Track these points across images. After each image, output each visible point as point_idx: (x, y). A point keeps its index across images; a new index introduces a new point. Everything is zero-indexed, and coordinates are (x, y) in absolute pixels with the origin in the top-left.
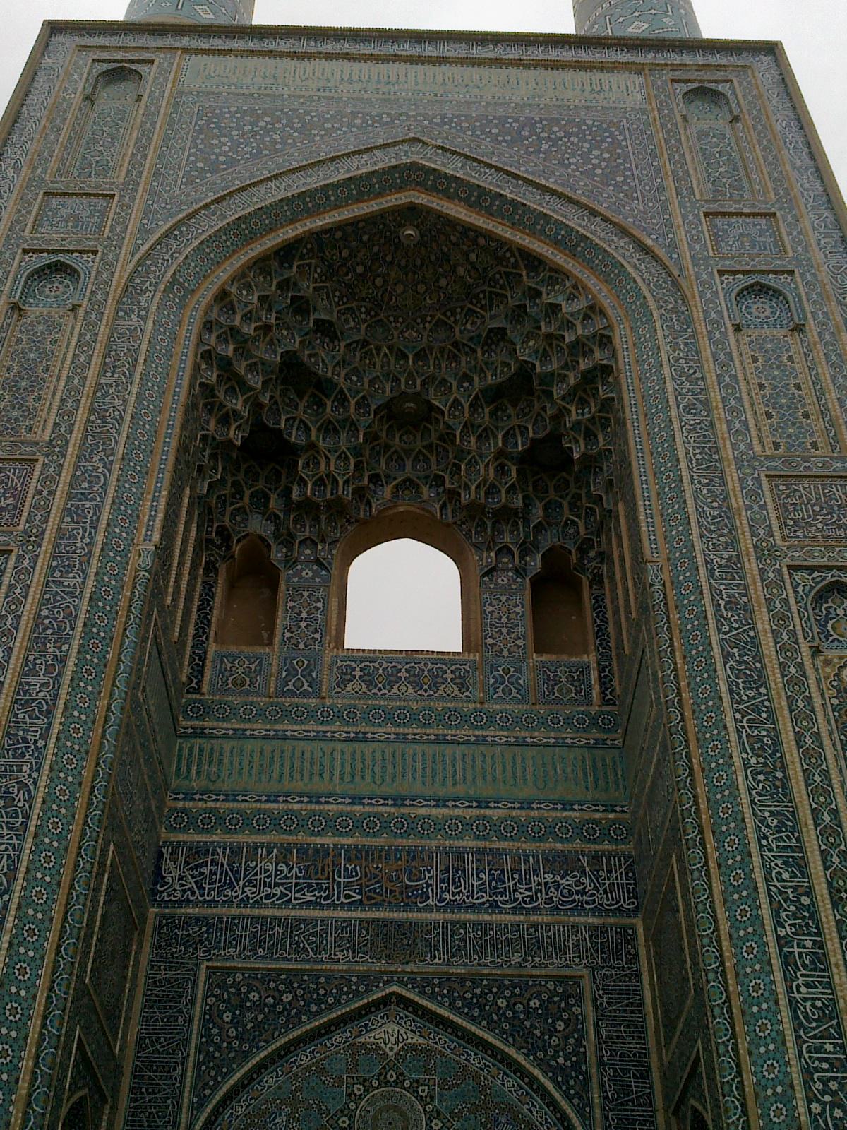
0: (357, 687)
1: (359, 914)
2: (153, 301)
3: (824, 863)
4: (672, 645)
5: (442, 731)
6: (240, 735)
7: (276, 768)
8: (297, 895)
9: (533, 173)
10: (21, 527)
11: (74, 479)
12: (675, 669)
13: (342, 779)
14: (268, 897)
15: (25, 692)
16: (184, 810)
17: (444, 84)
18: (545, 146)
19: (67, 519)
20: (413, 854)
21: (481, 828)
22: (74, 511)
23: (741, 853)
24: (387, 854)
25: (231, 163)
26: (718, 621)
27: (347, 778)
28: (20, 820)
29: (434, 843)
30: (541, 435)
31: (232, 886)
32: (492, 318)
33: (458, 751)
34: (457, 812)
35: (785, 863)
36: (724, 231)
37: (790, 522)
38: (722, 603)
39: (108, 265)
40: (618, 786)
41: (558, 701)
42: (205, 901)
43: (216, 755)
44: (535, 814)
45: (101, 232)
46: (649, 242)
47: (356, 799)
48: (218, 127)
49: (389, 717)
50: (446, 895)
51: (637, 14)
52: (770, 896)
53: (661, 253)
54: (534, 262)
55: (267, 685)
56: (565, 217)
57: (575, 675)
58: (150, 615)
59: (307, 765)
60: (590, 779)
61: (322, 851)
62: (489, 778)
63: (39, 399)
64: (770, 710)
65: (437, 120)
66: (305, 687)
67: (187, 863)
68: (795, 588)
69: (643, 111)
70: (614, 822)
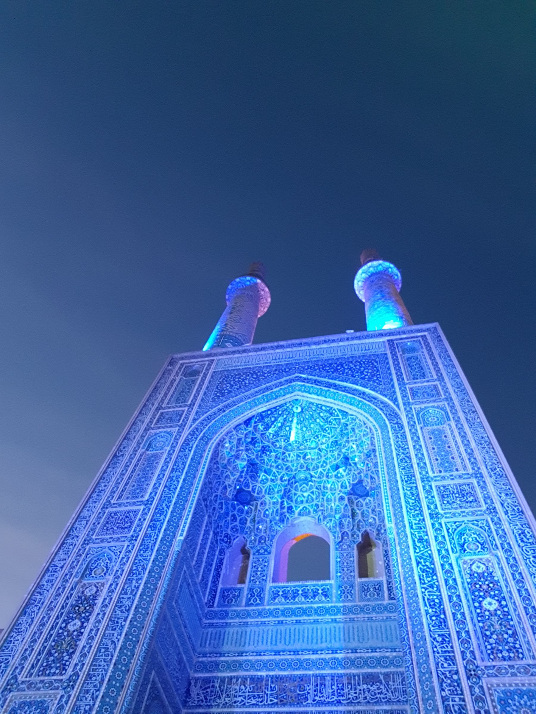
0: (280, 600)
1: (276, 709)
3: (463, 657)
4: (397, 561)
5: (316, 617)
7: (243, 639)
8: (249, 701)
10: (132, 533)
12: (399, 572)
13: (271, 643)
14: (235, 702)
15: (121, 602)
16: (201, 662)
18: (346, 371)
19: (149, 529)
20: (301, 678)
21: (333, 663)
22: (152, 526)
23: (425, 656)
24: (291, 678)
26: (414, 548)
27: (274, 643)
28: (110, 657)
29: (311, 673)
30: (355, 482)
31: (220, 698)
32: (332, 437)
33: (324, 626)
34: (322, 656)
35: (446, 659)
36: (417, 392)
37: (445, 502)
38: (416, 540)
39: (179, 433)
40: (397, 638)
41: (369, 600)
42: (207, 706)
43: (218, 635)
44: (358, 655)
47: (277, 653)
49: (293, 613)
50: (317, 698)
52: (438, 676)
54: (345, 414)
55: (241, 601)
56: (354, 394)
57: (377, 587)
58: (181, 568)
59: (256, 638)
60: (384, 636)
61: (261, 679)
62: (337, 639)
63: (147, 485)
66: (258, 601)
67: (201, 687)
68: (448, 530)
69: (386, 354)
70: (395, 657)
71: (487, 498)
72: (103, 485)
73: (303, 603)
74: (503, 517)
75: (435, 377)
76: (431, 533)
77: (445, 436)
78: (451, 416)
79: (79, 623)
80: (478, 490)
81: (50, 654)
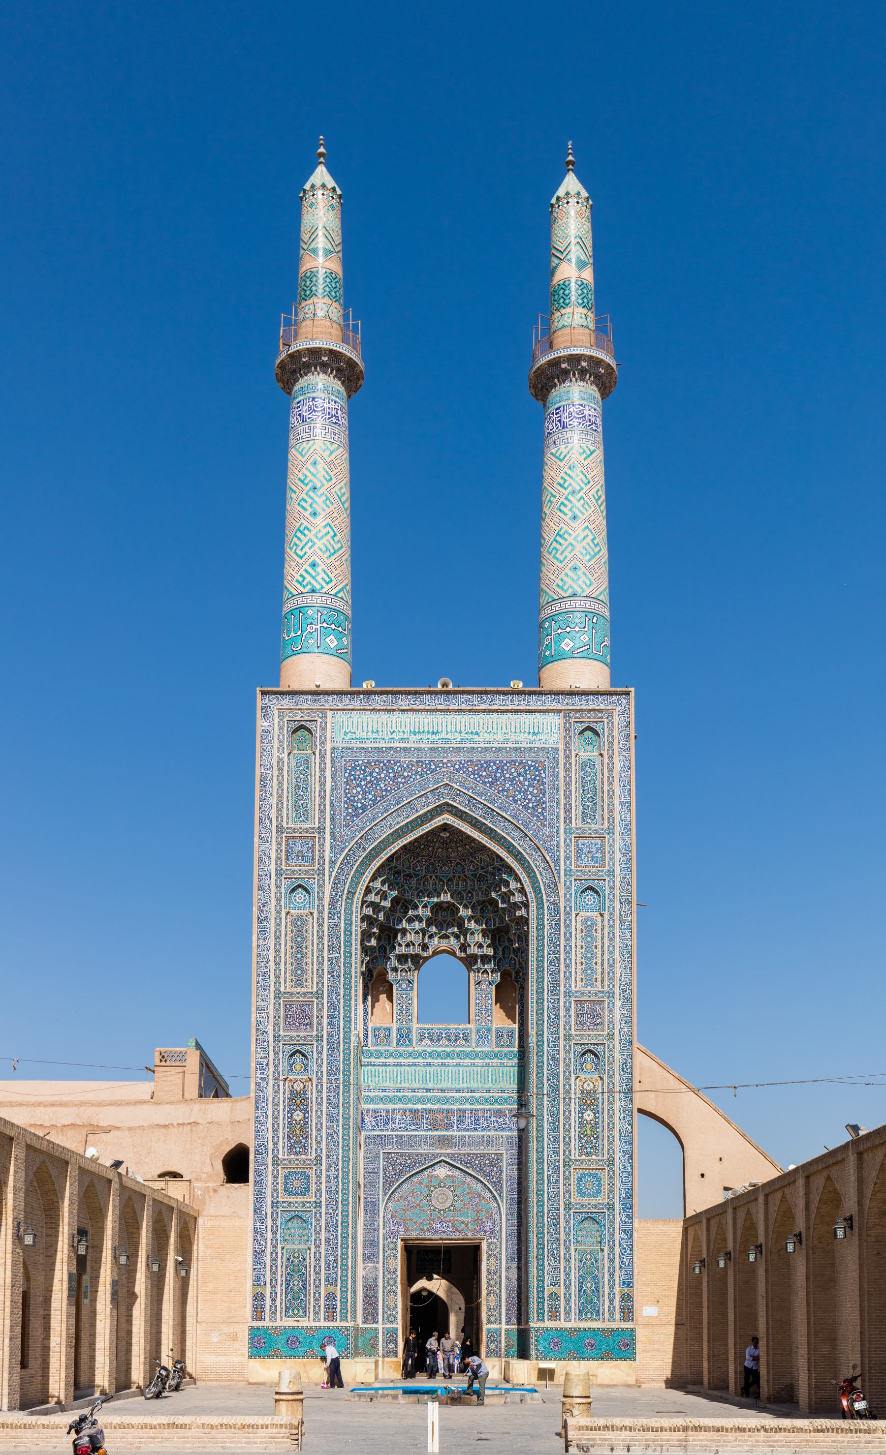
2: (342, 906)
6: (385, 1065)
9: (500, 808)
11: (328, 1007)
17: (460, 732)
25: (364, 808)
36: (581, 850)
39: (321, 886)
45: (313, 864)
46: (548, 858)
47: (428, 1090)
48: (355, 779)
51: (568, 629)
53: (552, 865)
55: (392, 1042)
56: (513, 838)
64: (558, 1101)
65: (457, 767)
69: (557, 749)
71: (611, 1022)
72: (262, 964)
73: (446, 1046)
74: (617, 1046)
75: (606, 825)
76: (562, 1055)
77: (596, 930)
78: (607, 905)
79: (301, 1114)
80: (606, 1013)
81: (289, 1137)
